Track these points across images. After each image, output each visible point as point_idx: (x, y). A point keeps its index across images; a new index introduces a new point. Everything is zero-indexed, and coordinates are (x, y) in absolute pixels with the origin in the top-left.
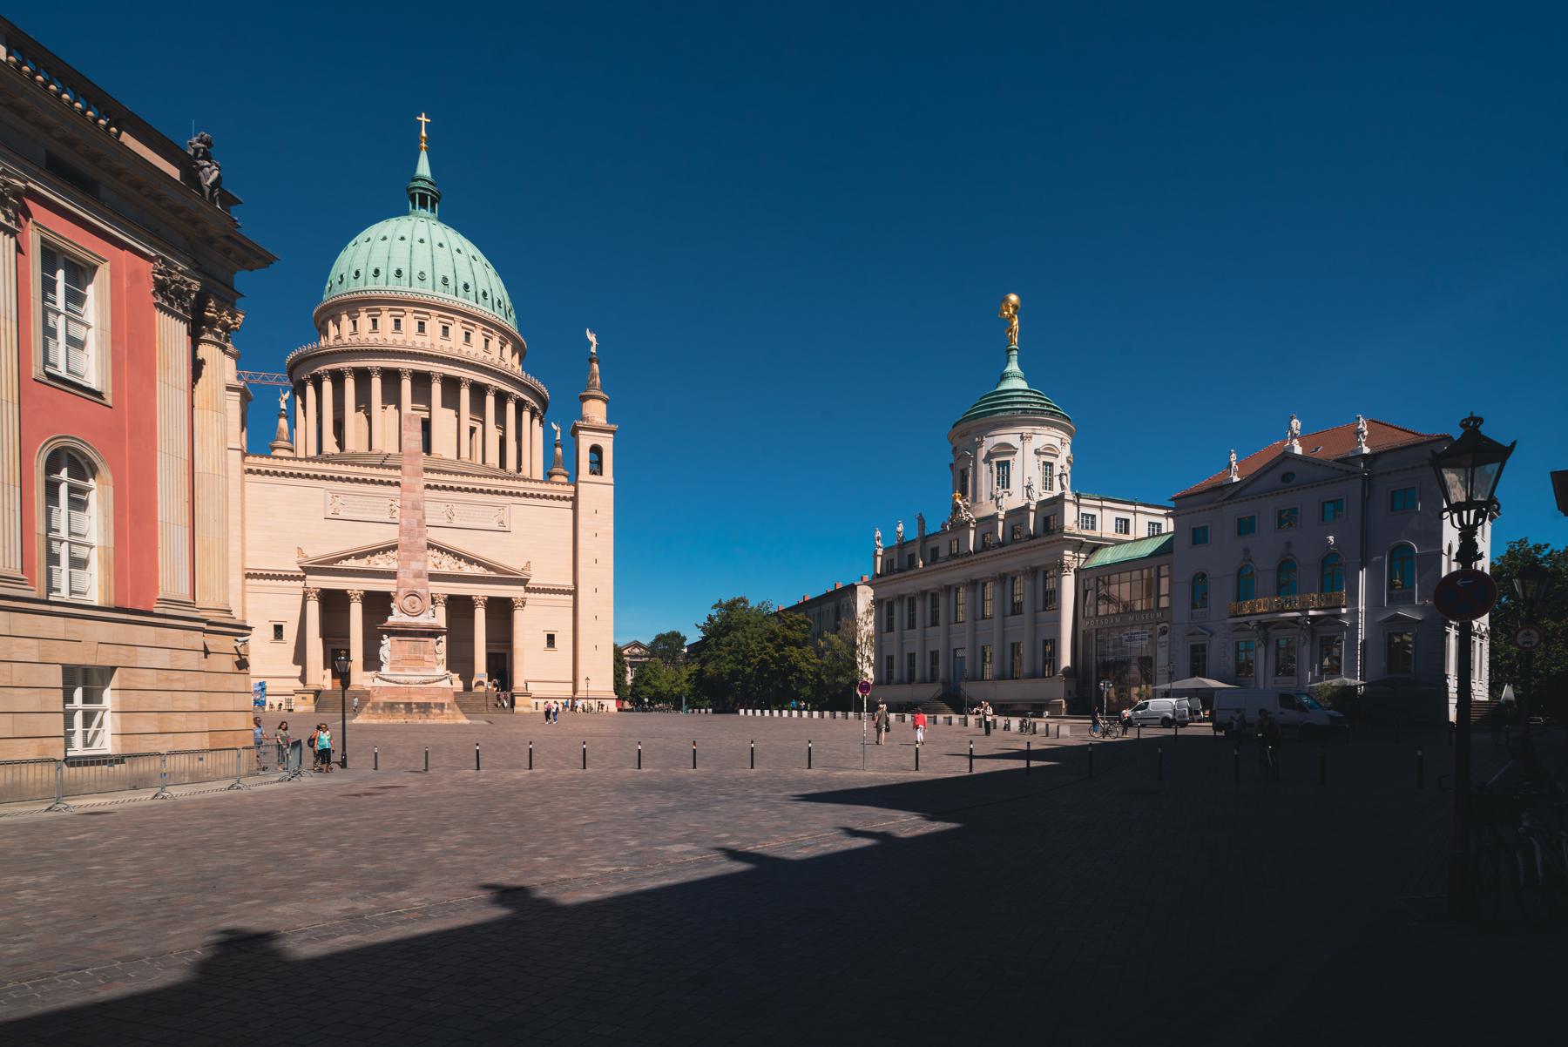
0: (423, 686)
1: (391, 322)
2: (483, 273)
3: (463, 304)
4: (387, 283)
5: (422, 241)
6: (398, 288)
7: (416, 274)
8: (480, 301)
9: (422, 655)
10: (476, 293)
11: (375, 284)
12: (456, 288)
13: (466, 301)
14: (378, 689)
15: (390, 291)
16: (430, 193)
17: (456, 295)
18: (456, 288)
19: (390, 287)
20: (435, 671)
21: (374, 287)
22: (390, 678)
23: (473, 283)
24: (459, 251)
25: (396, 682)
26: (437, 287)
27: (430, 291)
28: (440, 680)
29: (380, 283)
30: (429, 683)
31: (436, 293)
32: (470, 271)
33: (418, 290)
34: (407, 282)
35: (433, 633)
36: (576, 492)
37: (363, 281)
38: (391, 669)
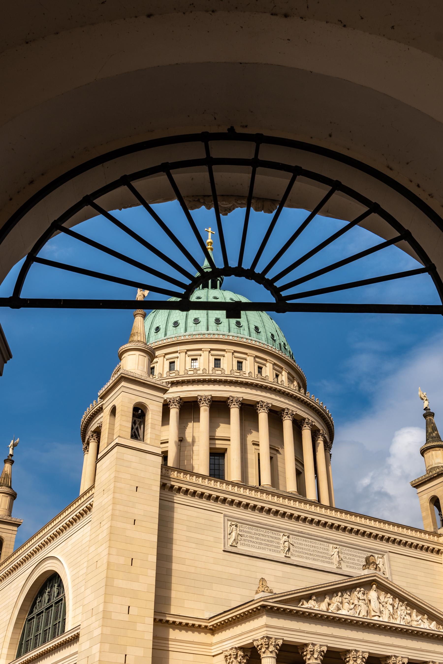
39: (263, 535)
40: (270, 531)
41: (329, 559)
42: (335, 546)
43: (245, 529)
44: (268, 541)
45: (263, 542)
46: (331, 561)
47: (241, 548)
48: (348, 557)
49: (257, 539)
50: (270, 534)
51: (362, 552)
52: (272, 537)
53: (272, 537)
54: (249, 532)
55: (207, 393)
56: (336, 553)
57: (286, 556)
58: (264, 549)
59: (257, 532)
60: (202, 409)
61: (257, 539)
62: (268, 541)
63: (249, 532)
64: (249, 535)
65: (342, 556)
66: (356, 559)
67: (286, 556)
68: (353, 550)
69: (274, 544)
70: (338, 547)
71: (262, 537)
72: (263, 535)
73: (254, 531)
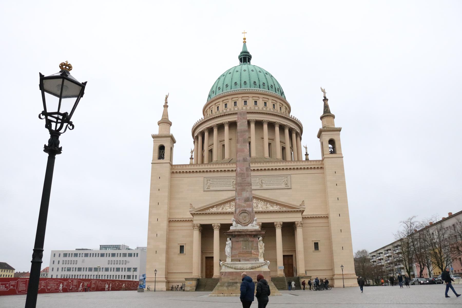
0: (252, 270)
1: (233, 103)
2: (270, 78)
3: (263, 91)
4: (231, 88)
5: (245, 71)
6: (236, 89)
7: (243, 82)
8: (270, 89)
9: (250, 250)
10: (268, 86)
11: (226, 90)
12: (259, 85)
13: (264, 90)
14: (224, 273)
15: (232, 91)
16: (247, 56)
17: (260, 88)
18: (259, 85)
19: (232, 90)
20: (258, 260)
21: (226, 91)
22: (231, 266)
23: (266, 82)
24: (260, 72)
25: (235, 269)
26: (252, 86)
27: (249, 88)
28: (262, 266)
29: (229, 89)
30: (255, 268)
31: (251, 88)
32: (265, 78)
33: (244, 88)
34: (239, 86)
35: (254, 235)
36: (323, 164)
37: (222, 90)
38: (232, 260)
39: (223, 181)
40: (226, 179)
41: (257, 184)
42: (260, 178)
43: (214, 181)
44: (225, 183)
45: (222, 184)
46: (257, 185)
47: (211, 188)
48: (267, 181)
49: (220, 183)
50: (226, 180)
51: (275, 177)
52: (227, 181)
53: (227, 181)
54: (216, 182)
55: (215, 123)
56: (260, 181)
57: (233, 188)
58: (223, 187)
59: (220, 181)
60: (214, 130)
61: (220, 183)
62: (225, 183)
63: (216, 182)
64: (216, 182)
65: (263, 182)
66: (271, 181)
67: (233, 188)
68: (270, 178)
69: (228, 184)
70: (261, 178)
71: (222, 182)
72: (223, 181)
73: (218, 181)
